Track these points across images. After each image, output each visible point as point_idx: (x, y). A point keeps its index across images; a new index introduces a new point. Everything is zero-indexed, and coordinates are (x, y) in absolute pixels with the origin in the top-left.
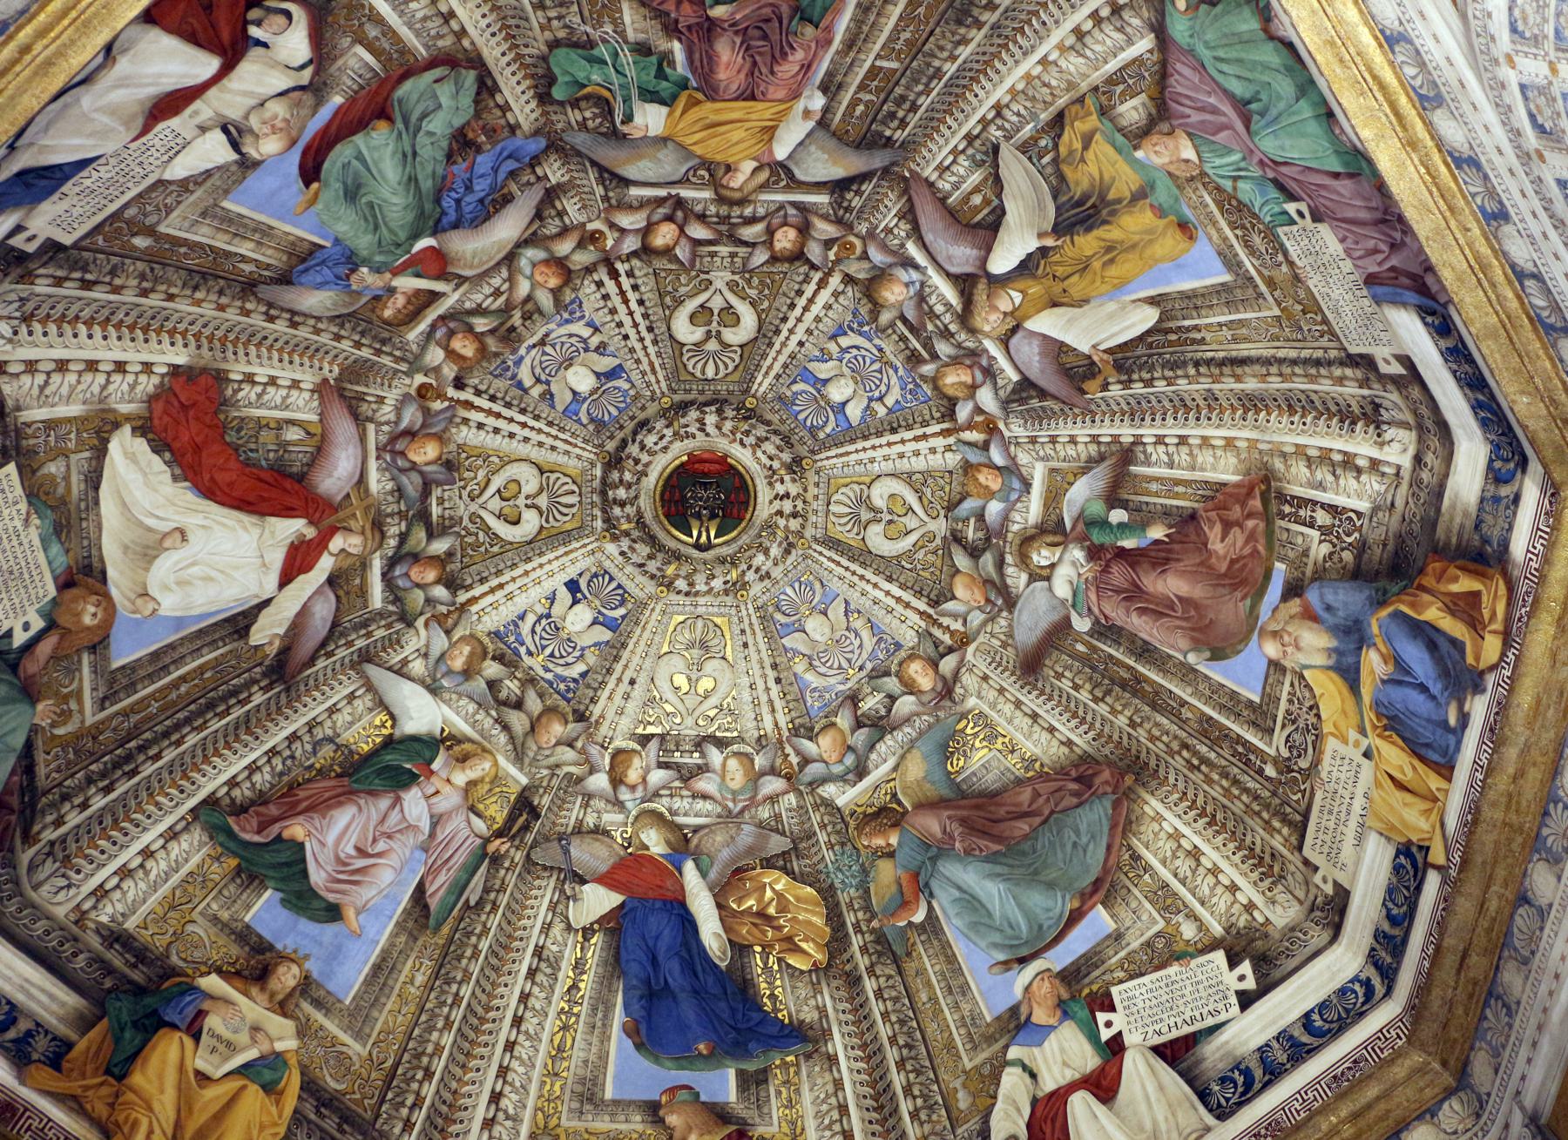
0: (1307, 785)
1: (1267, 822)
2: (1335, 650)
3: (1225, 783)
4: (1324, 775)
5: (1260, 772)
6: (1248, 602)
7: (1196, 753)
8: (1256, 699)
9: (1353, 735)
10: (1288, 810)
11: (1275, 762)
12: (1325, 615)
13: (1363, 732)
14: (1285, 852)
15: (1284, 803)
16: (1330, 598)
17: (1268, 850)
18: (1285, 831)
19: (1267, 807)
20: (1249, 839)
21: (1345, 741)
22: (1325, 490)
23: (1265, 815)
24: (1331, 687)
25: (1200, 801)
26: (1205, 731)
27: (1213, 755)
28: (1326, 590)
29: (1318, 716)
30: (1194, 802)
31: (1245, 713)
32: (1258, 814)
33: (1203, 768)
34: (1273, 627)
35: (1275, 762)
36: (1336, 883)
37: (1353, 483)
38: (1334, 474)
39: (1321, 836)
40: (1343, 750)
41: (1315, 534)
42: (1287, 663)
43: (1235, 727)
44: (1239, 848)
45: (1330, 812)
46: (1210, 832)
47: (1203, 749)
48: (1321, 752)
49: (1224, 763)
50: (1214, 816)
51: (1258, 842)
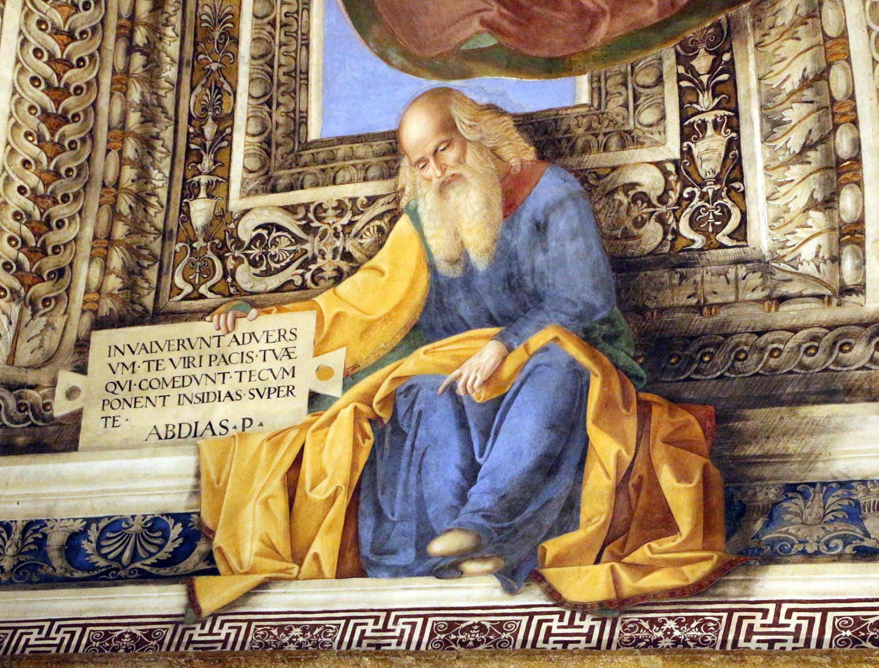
0: (212, 299)
1: (109, 237)
2: (469, 271)
3: (134, 118)
4: (244, 326)
5: (190, 191)
6: (488, 41)
7: (156, 30)
8: (314, 132)
9: (337, 360)
10: (152, 274)
11: (221, 216)
12: (524, 225)
13: (351, 378)
14: (78, 295)
15: (158, 259)
16: (560, 225)
17: (64, 259)
18: (114, 283)
19: (136, 229)
20: (61, 211)
21: (320, 348)
22: (766, 138)
23: (120, 230)
24: (400, 287)
25: (75, 77)
26: (208, 39)
27: (170, 72)
28: (571, 209)
29: (339, 277)
30: (67, 64)
31: (278, 116)
32: (115, 215)
33: (138, 60)
34: (461, 116)
35: (221, 216)
36: (77, 416)
37: (800, 196)
38: (807, 147)
39: (140, 358)
40: (304, 345)
41: (672, 148)
42: (406, 175)
43: (243, 100)
44: (35, 197)
45: (188, 362)
46: (33, 122)
47: (171, 47)
48: (280, 306)
49: (168, 102)
50: (65, 119)
51: (68, 233)
